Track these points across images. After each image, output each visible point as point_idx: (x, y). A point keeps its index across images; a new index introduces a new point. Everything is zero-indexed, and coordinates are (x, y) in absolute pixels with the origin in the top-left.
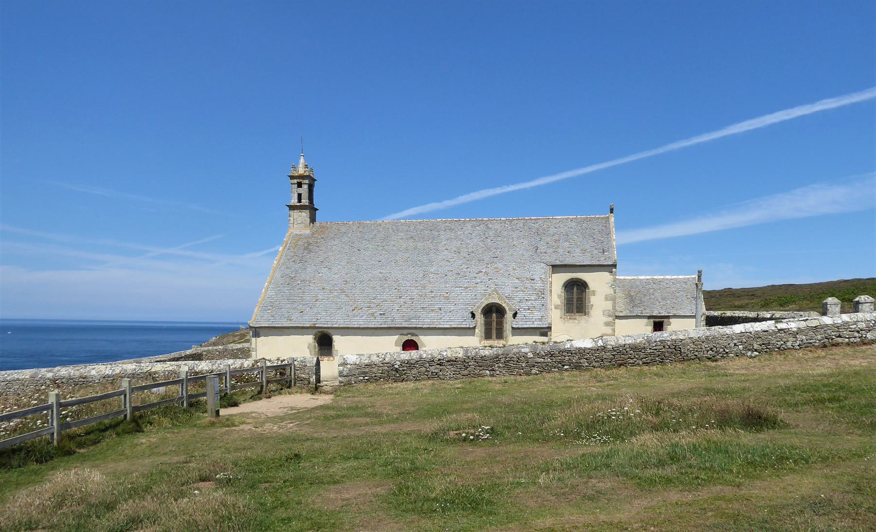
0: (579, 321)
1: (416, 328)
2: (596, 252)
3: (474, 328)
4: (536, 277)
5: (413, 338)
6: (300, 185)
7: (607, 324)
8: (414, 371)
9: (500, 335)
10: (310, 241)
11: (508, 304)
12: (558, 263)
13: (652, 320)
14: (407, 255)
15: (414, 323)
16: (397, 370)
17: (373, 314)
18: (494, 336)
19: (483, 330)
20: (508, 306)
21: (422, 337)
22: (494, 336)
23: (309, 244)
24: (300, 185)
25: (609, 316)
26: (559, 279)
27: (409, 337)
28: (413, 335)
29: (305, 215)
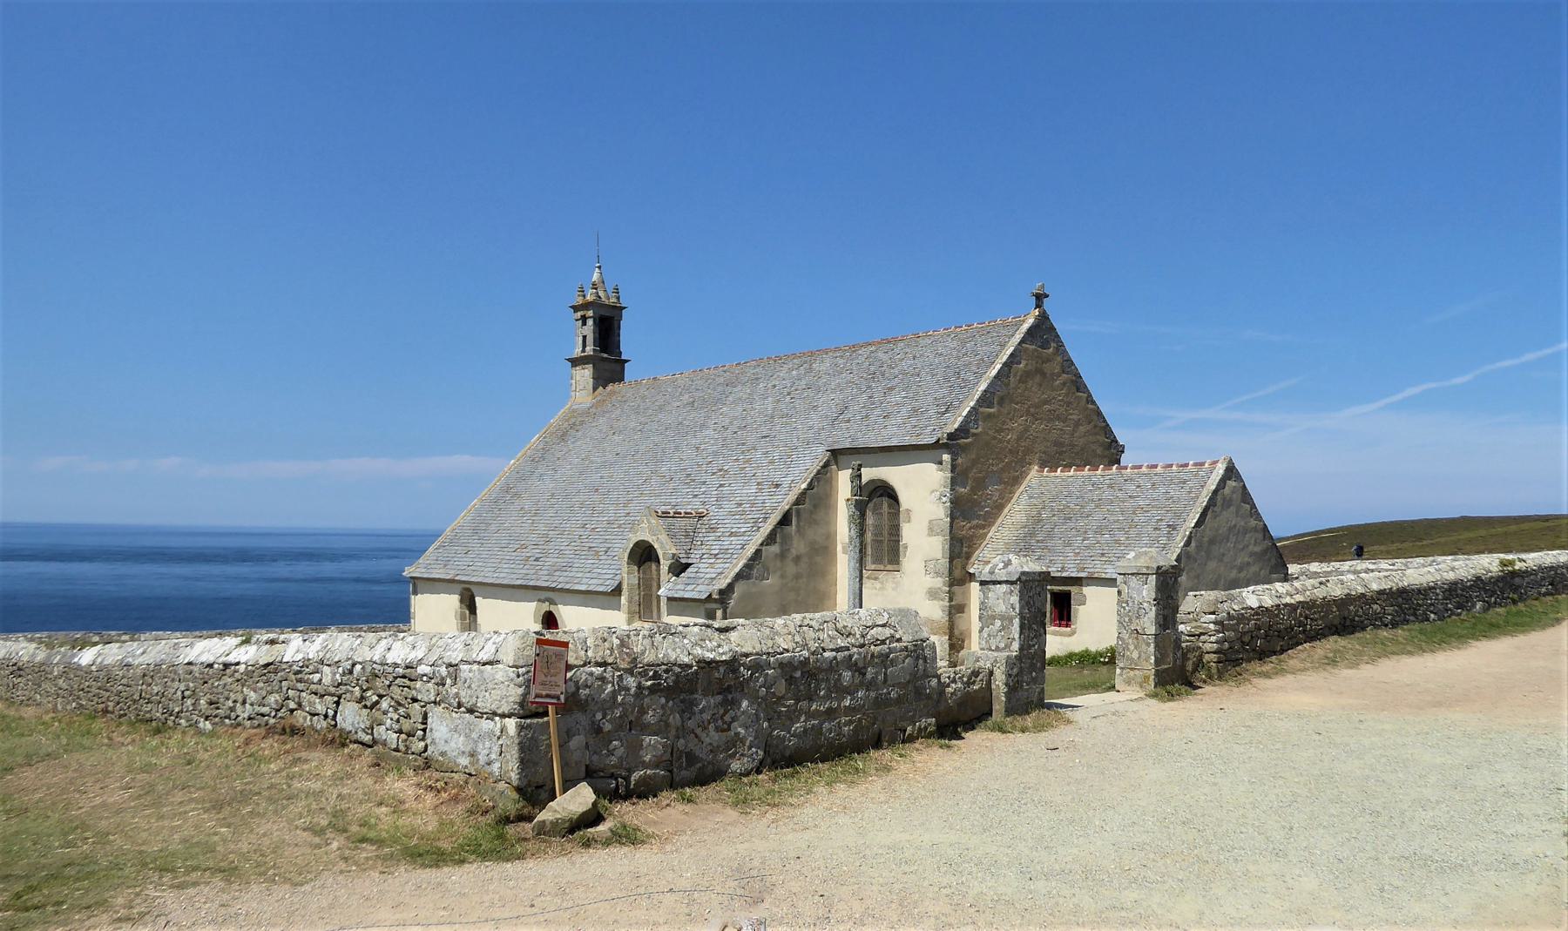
0: (882, 583)
1: (553, 590)
6: (584, 319)
15: (560, 581)
20: (661, 548)
24: (584, 319)
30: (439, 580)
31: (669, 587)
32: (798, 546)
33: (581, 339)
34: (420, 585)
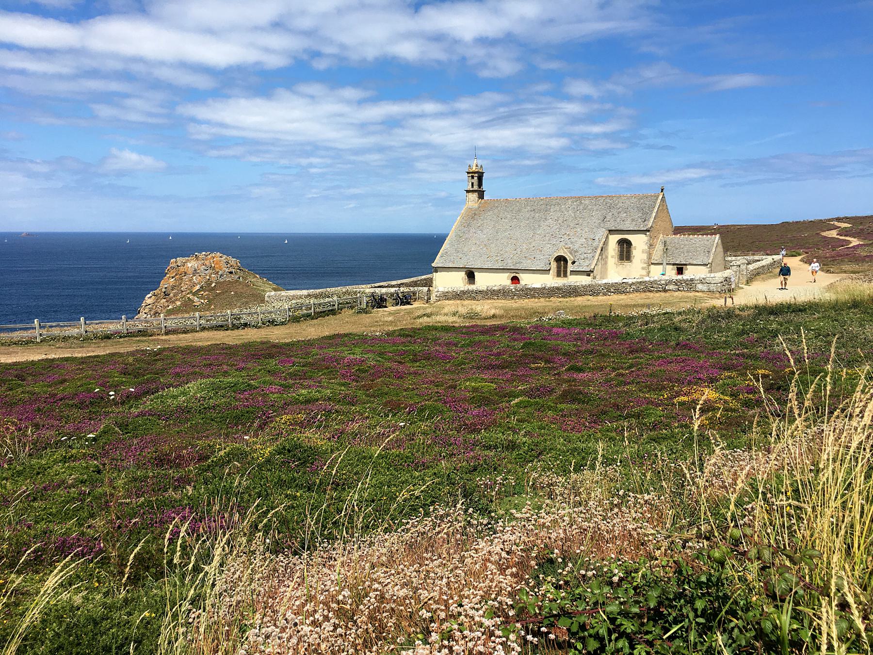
2: (640, 221)
3: (549, 270)
4: (597, 238)
5: (517, 275)
6: (473, 177)
7: (643, 268)
8: (466, 296)
9: (565, 275)
10: (476, 212)
11: (569, 256)
12: (613, 228)
13: (675, 266)
14: (528, 222)
16: (458, 295)
17: (497, 260)
18: (562, 275)
19: (556, 271)
21: (521, 274)
22: (562, 275)
23: (475, 214)
24: (473, 177)
25: (645, 263)
26: (614, 239)
27: (514, 275)
28: (517, 273)
29: (475, 195)
30: (452, 268)
31: (570, 268)
32: (604, 257)
33: (471, 183)
34: (439, 269)
